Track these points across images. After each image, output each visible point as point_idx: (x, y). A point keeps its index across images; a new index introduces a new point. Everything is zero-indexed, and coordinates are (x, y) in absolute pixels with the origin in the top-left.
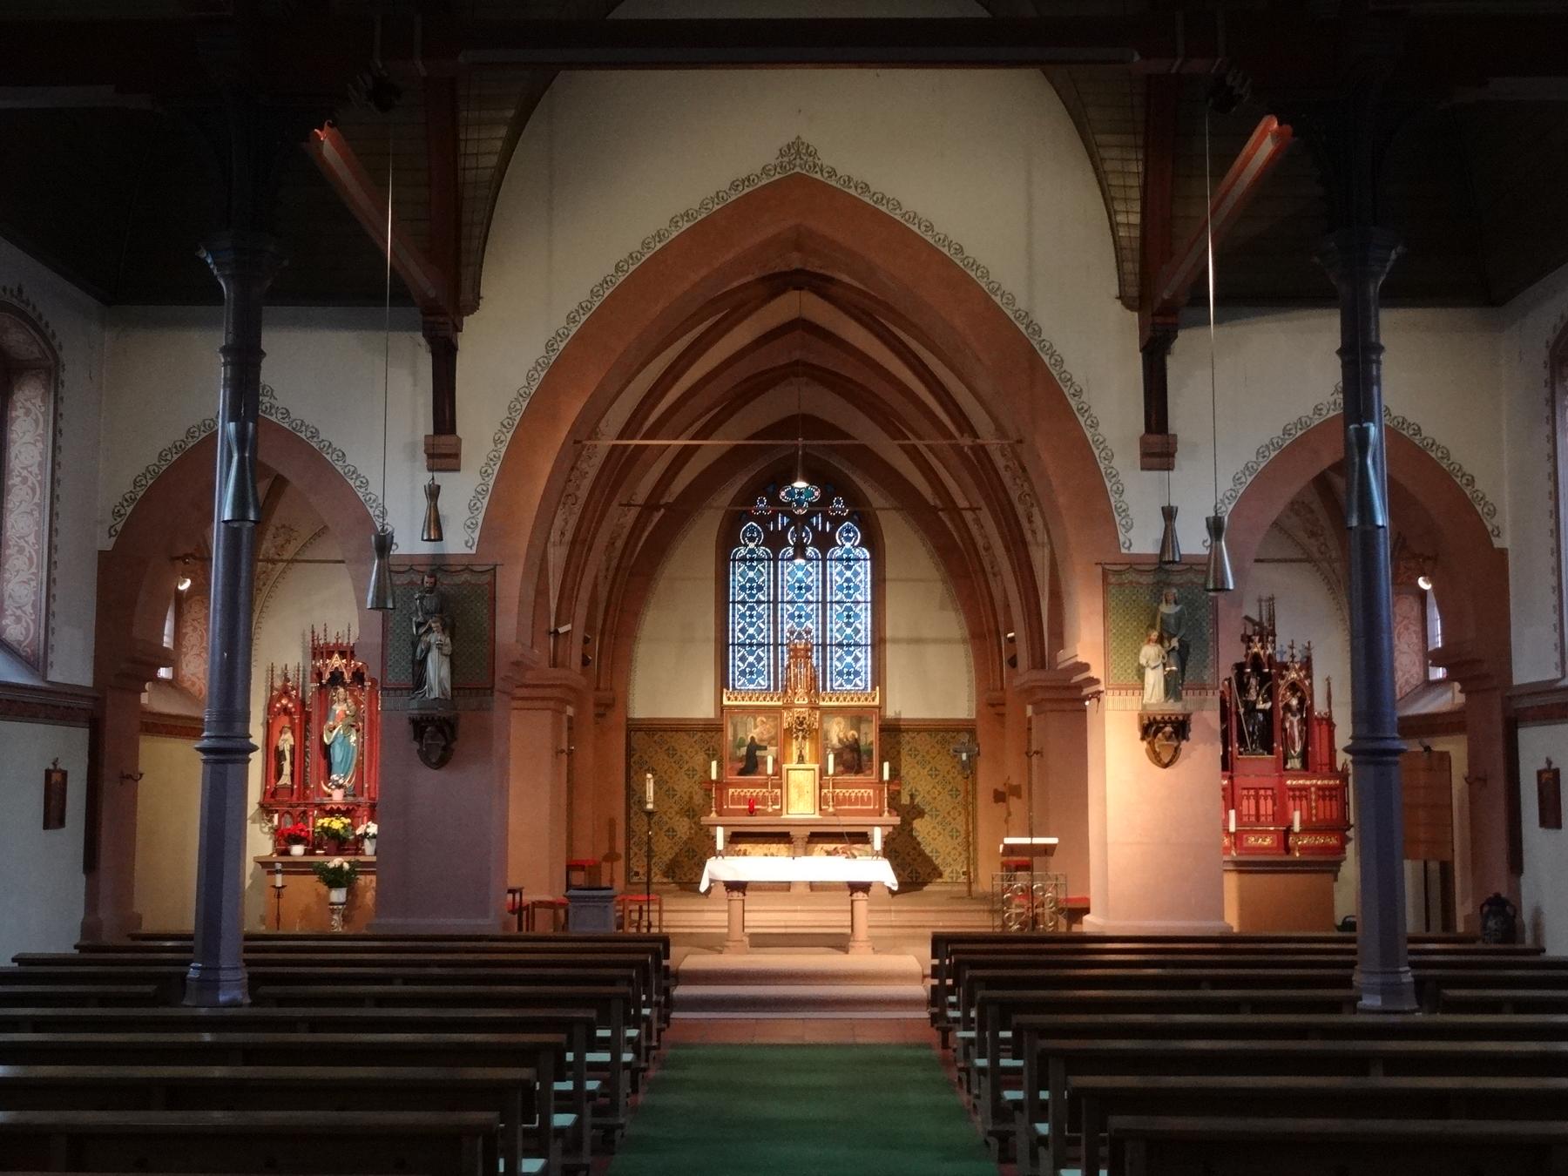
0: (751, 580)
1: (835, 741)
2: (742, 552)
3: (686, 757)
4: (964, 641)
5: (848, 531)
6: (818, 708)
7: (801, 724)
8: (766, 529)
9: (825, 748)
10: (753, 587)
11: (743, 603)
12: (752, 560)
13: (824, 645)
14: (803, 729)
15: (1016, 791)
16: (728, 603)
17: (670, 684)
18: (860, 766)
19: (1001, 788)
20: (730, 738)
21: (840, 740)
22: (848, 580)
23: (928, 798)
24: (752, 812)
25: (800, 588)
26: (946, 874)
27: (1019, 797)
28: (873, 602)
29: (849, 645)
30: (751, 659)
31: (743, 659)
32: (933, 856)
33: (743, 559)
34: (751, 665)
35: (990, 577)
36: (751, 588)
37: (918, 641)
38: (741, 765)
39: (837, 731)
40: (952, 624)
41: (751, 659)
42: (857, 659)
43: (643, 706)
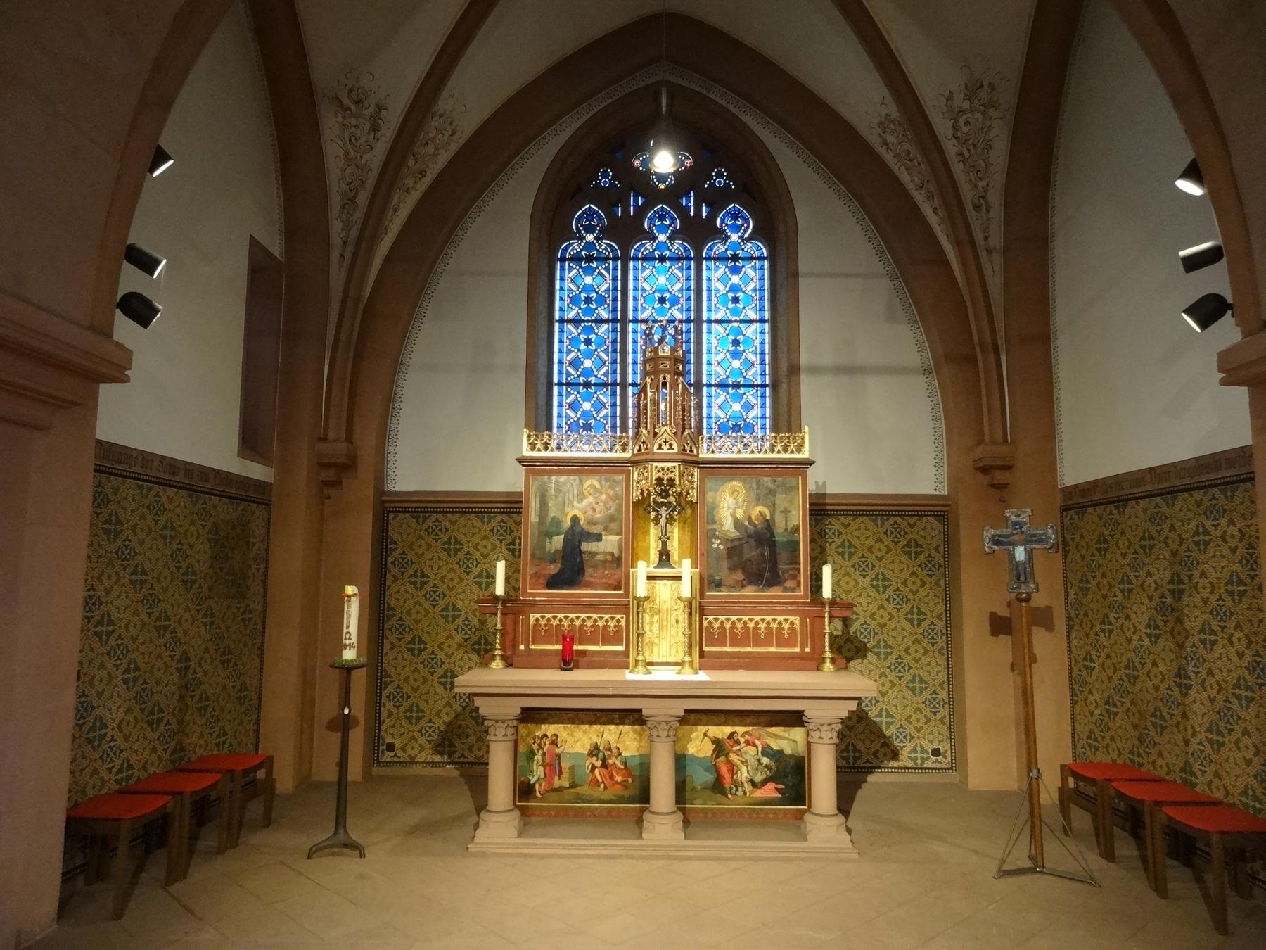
0: (587, 288)
1: (728, 525)
2: (576, 246)
3: (477, 555)
4: (926, 371)
5: (735, 217)
6: (697, 463)
7: (665, 494)
8: (611, 215)
9: (710, 536)
10: (590, 299)
11: (576, 322)
12: (589, 259)
13: (698, 386)
14: (668, 501)
15: (1043, 618)
17: (456, 434)
18: (774, 569)
19: (1003, 611)
20: (533, 518)
21: (737, 524)
22: (734, 288)
23: (873, 625)
24: (568, 661)
25: (662, 300)
26: (904, 754)
27: (1050, 627)
28: (774, 322)
29: (737, 386)
30: (587, 406)
31: (574, 406)
32: (883, 722)
33: (576, 259)
34: (586, 414)
35: (983, 255)
36: (588, 300)
38: (554, 569)
39: (731, 506)
40: (905, 343)
41: (587, 406)
42: (748, 407)
43: (406, 477)
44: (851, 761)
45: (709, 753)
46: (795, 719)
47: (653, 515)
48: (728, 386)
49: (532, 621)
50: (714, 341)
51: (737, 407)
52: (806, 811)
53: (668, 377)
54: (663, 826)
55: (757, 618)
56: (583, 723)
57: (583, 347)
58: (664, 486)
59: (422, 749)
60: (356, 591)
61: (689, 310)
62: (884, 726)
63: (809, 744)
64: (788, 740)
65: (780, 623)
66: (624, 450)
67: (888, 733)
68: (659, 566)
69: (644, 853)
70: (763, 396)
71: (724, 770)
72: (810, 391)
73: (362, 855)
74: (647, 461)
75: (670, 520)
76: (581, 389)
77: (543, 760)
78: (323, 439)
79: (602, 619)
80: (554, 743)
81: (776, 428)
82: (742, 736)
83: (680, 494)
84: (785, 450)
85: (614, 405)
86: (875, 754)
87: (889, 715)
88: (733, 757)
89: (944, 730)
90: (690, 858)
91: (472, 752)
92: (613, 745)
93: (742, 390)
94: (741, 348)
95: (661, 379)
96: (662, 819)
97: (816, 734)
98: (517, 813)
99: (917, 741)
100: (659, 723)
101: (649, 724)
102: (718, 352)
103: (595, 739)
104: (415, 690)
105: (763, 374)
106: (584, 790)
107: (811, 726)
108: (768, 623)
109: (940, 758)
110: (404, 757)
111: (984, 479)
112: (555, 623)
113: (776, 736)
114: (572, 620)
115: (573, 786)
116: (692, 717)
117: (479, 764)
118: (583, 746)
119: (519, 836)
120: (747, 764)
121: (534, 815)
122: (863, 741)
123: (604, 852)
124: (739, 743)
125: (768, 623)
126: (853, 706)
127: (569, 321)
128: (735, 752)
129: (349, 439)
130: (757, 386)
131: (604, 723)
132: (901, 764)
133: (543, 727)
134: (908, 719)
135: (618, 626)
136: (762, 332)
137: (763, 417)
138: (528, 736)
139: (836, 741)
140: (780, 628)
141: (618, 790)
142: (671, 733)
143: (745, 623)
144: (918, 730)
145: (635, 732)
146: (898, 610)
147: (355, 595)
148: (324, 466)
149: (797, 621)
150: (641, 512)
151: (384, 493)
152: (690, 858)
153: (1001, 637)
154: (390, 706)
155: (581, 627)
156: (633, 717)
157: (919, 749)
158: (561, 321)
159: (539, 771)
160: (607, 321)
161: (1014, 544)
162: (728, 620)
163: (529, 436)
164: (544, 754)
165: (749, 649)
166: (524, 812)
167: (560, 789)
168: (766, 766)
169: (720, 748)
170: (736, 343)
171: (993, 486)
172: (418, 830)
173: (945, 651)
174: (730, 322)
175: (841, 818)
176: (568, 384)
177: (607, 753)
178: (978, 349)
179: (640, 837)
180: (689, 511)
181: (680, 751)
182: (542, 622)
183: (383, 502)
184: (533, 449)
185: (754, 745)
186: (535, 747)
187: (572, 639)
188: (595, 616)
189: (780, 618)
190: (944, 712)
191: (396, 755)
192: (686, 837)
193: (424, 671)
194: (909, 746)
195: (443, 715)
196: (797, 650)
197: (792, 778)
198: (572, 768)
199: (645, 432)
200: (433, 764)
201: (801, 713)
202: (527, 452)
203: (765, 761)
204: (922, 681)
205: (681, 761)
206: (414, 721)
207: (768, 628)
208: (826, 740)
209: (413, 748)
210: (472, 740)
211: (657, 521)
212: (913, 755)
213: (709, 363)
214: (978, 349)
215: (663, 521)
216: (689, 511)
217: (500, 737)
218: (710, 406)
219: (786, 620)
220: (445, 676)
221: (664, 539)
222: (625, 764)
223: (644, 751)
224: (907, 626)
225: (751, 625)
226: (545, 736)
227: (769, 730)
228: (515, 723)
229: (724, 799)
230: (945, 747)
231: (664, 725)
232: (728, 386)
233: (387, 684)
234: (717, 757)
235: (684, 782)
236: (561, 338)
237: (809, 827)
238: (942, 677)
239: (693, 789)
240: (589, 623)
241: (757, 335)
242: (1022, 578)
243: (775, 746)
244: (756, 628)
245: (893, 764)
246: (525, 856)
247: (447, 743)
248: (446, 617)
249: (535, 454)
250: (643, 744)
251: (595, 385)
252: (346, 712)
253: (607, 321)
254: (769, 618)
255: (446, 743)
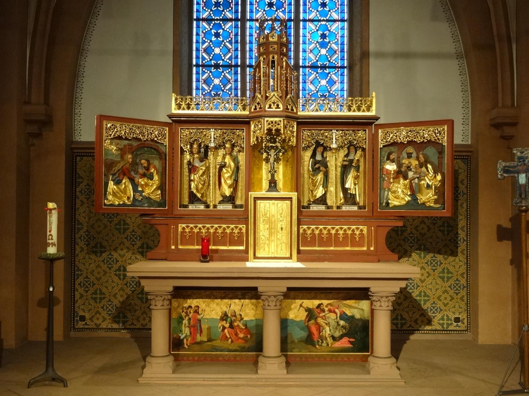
4: (458, 56)
11: (208, 20)
16: (190, 20)
19: (507, 224)
24: (205, 256)
26: (435, 321)
28: (351, 21)
29: (324, 67)
30: (217, 81)
32: (421, 300)
37: (406, 55)
40: (444, 36)
41: (217, 81)
42: (332, 83)
44: (399, 326)
45: (304, 318)
46: (362, 294)
47: (265, 155)
48: (317, 67)
49: (180, 229)
50: (307, 34)
51: (324, 82)
52: (369, 356)
53: (276, 57)
54: (272, 366)
55: (337, 227)
56: (216, 298)
57: (214, 39)
58: (273, 134)
59: (104, 320)
60: (55, 206)
61: (290, 12)
62: (422, 303)
63: (372, 311)
64: (358, 309)
65: (353, 231)
66: (244, 109)
67: (425, 307)
68: (268, 191)
69: (259, 383)
70: (342, 75)
71: (314, 330)
72: (376, 69)
73: (65, 386)
74: (261, 117)
75: (277, 160)
76: (213, 70)
77: (189, 323)
78: (28, 103)
79: (230, 228)
80: (196, 312)
81: (351, 93)
82: (326, 306)
83: (284, 141)
84: (359, 110)
85: (236, 81)
86: (416, 321)
87: (426, 295)
88: (320, 320)
89: (464, 306)
90: (291, 386)
91: (139, 321)
92: (237, 313)
93: (327, 71)
94: (327, 40)
95: (271, 56)
96: (272, 361)
97: (378, 304)
98: (171, 358)
99: (445, 311)
100: (270, 296)
101: (262, 297)
102: (311, 43)
103: (225, 309)
104: (98, 279)
105: (342, 59)
106: (218, 343)
107: (374, 298)
108: (345, 230)
109: (459, 324)
110: (92, 325)
111: (497, 133)
112: (196, 230)
113: (350, 307)
114: (208, 229)
115: (210, 340)
116: (293, 293)
117: (144, 329)
118: (217, 314)
119: (174, 372)
120: (330, 325)
121: (183, 360)
122: (408, 312)
123: (233, 383)
124: (323, 311)
125: (345, 230)
126: (403, 284)
127: (204, 20)
128: (322, 317)
129: (47, 102)
130: (338, 67)
131: (231, 298)
132: (433, 328)
133: (189, 301)
134: (439, 298)
135: (240, 233)
136: (342, 28)
137: (342, 90)
138: (178, 307)
139: (391, 308)
140: (353, 234)
141: (241, 343)
142: (278, 304)
143: (329, 230)
144: (446, 305)
145: (253, 304)
146: (434, 224)
147: (55, 209)
148: (29, 122)
149: (365, 229)
150: (256, 153)
151: (73, 142)
152: (291, 386)
153: (505, 242)
154: (81, 290)
155: (215, 233)
156: (251, 293)
157: (445, 318)
158: (198, 20)
159: (186, 331)
160: (231, 20)
161: (518, 173)
162: (317, 228)
163: (176, 99)
164: (190, 319)
165: (332, 248)
166: (177, 358)
167: (200, 343)
168: (342, 327)
169: (311, 314)
170: (323, 36)
171: (503, 137)
172: (102, 370)
173: (465, 252)
174: (319, 21)
175: (394, 360)
176: (203, 66)
177: (233, 318)
178: (496, 39)
179: (257, 372)
180: (290, 153)
181: (283, 317)
182: (187, 230)
183: (72, 149)
184: (179, 108)
185: (335, 312)
186: (183, 314)
187: (208, 241)
188: (224, 226)
189: (354, 227)
190: (463, 293)
191: (86, 323)
192: (288, 373)
193: (105, 267)
194: (439, 316)
195: (118, 296)
196: (365, 249)
197: (360, 334)
198: (209, 329)
199: (259, 96)
200: (112, 329)
201: (367, 289)
202: (175, 111)
203: (342, 323)
204: (449, 272)
205: (284, 323)
206: (98, 300)
207: (345, 234)
208: (384, 308)
209: (98, 319)
210: (138, 313)
211: (267, 160)
212: (441, 322)
213: (304, 51)
214: (496, 39)
215: (272, 160)
216: (290, 153)
217: (159, 307)
218: (305, 82)
219: (357, 229)
220: (119, 270)
221: (273, 172)
222: (246, 325)
223: (259, 317)
224: (440, 234)
225: (333, 232)
226: (190, 307)
227: (344, 302)
228: (169, 297)
229: (313, 349)
230: (463, 316)
231: (272, 298)
232: (317, 67)
233: (79, 276)
234: (309, 321)
235: (286, 337)
236: (200, 31)
237: (372, 365)
238: (463, 269)
239: (293, 342)
240: (220, 231)
241: (340, 31)
242: (523, 196)
243: (349, 313)
244: (337, 234)
245: (428, 328)
246: (178, 385)
247: (121, 315)
248: (119, 230)
249: (181, 112)
250: (258, 312)
251: (223, 66)
252: (51, 289)
253: (231, 20)
254: (345, 227)
255: (121, 315)
